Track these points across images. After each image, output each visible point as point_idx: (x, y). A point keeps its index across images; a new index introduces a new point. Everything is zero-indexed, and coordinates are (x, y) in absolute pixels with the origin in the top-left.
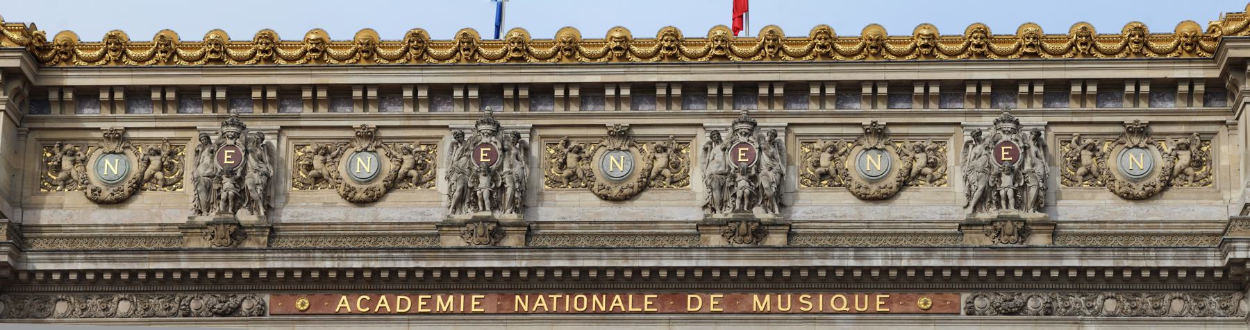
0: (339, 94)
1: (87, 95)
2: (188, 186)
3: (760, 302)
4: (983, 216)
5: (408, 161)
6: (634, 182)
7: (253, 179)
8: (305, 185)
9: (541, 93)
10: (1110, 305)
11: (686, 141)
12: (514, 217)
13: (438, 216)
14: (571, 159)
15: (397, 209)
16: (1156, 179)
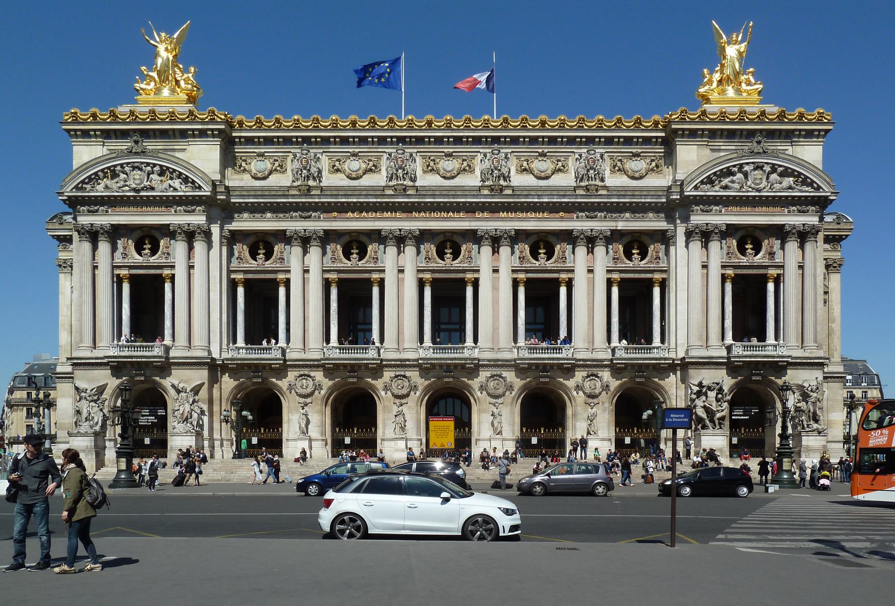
0: (344, 141)
1: (250, 141)
2: (289, 172)
3: (503, 215)
4: (583, 184)
5: (371, 164)
6: (455, 172)
7: (314, 170)
8: (332, 173)
9: (420, 141)
10: (627, 215)
11: (473, 157)
12: (411, 184)
13: (384, 184)
14: (432, 164)
15: (367, 181)
16: (643, 172)
